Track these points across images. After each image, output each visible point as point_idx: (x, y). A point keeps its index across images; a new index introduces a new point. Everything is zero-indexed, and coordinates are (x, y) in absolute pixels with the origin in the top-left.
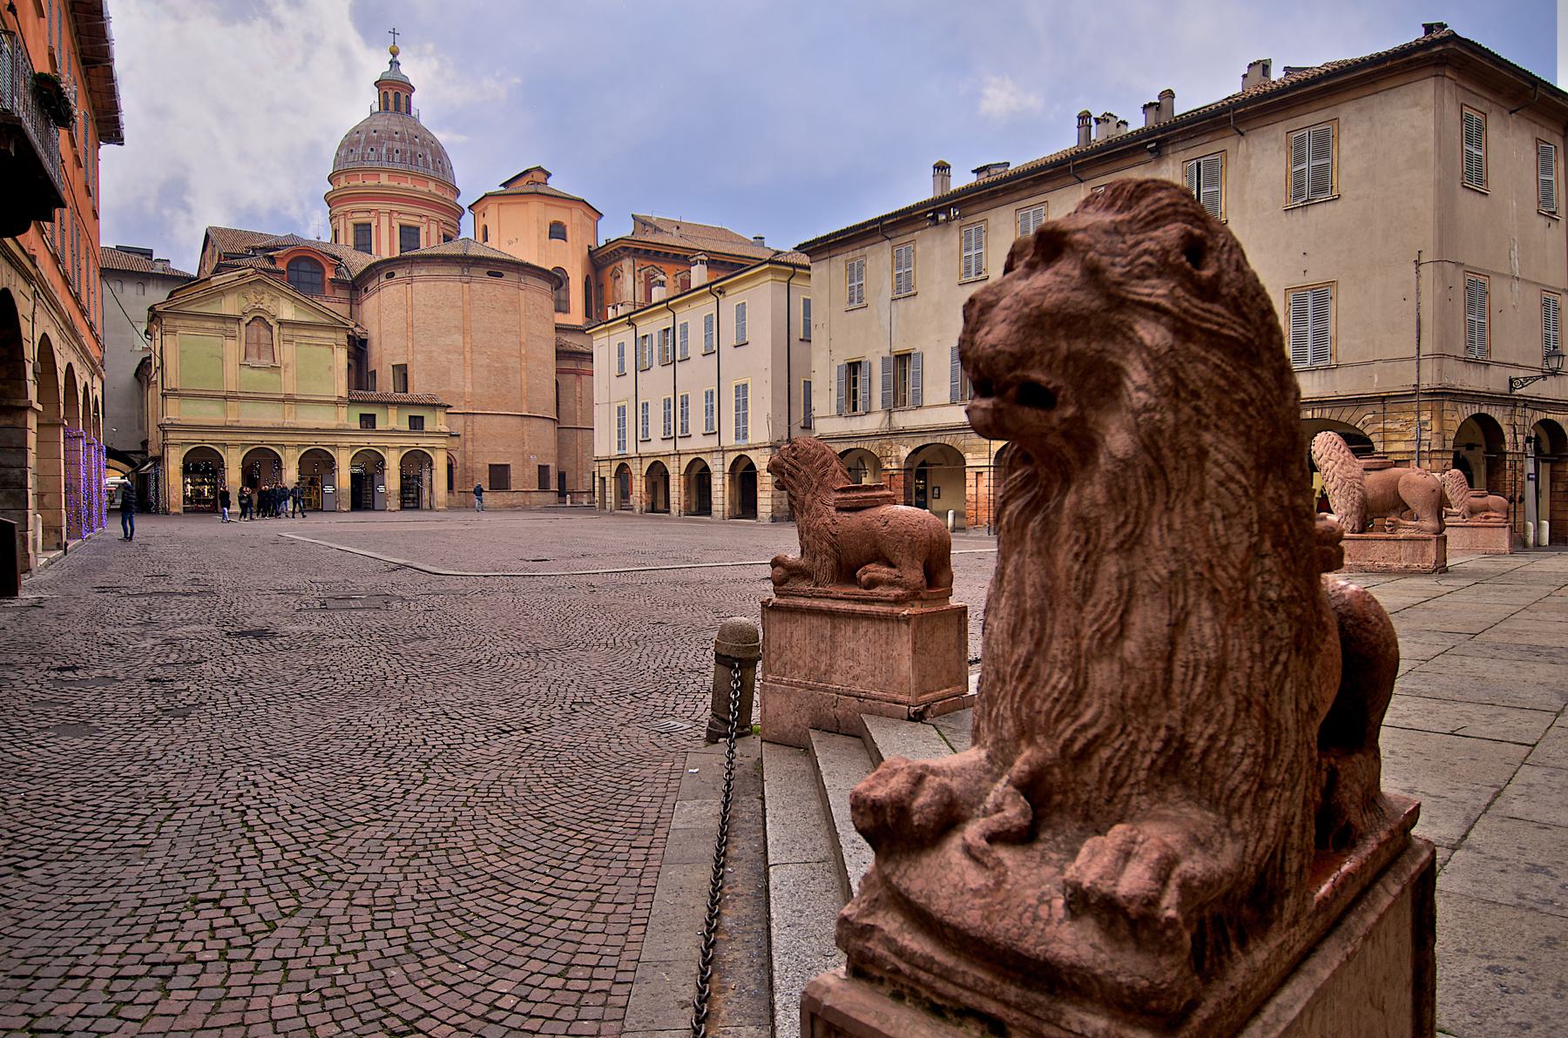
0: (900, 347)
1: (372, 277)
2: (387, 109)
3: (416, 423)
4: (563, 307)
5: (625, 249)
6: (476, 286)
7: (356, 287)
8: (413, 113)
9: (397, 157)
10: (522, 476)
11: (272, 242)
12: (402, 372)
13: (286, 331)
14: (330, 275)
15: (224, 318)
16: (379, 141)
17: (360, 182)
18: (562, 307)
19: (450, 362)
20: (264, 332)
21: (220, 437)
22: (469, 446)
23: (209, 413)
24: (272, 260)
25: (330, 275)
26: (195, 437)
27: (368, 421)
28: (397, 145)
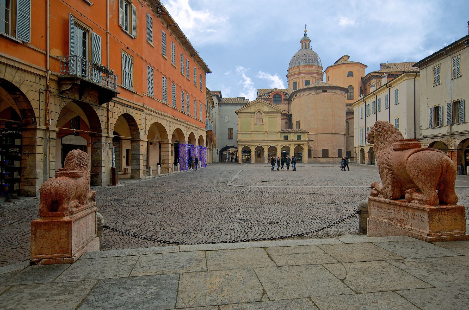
0: (455, 99)
1: (292, 97)
3: (299, 138)
4: (352, 98)
5: (373, 76)
6: (319, 95)
7: (289, 100)
10: (333, 152)
11: (270, 91)
12: (298, 122)
13: (266, 114)
14: (283, 98)
15: (251, 113)
16: (300, 58)
18: (351, 98)
20: (261, 115)
21: (250, 143)
22: (316, 144)
23: (247, 138)
24: (269, 96)
25: (283, 98)
26: (244, 144)
27: (286, 138)
28: (304, 58)
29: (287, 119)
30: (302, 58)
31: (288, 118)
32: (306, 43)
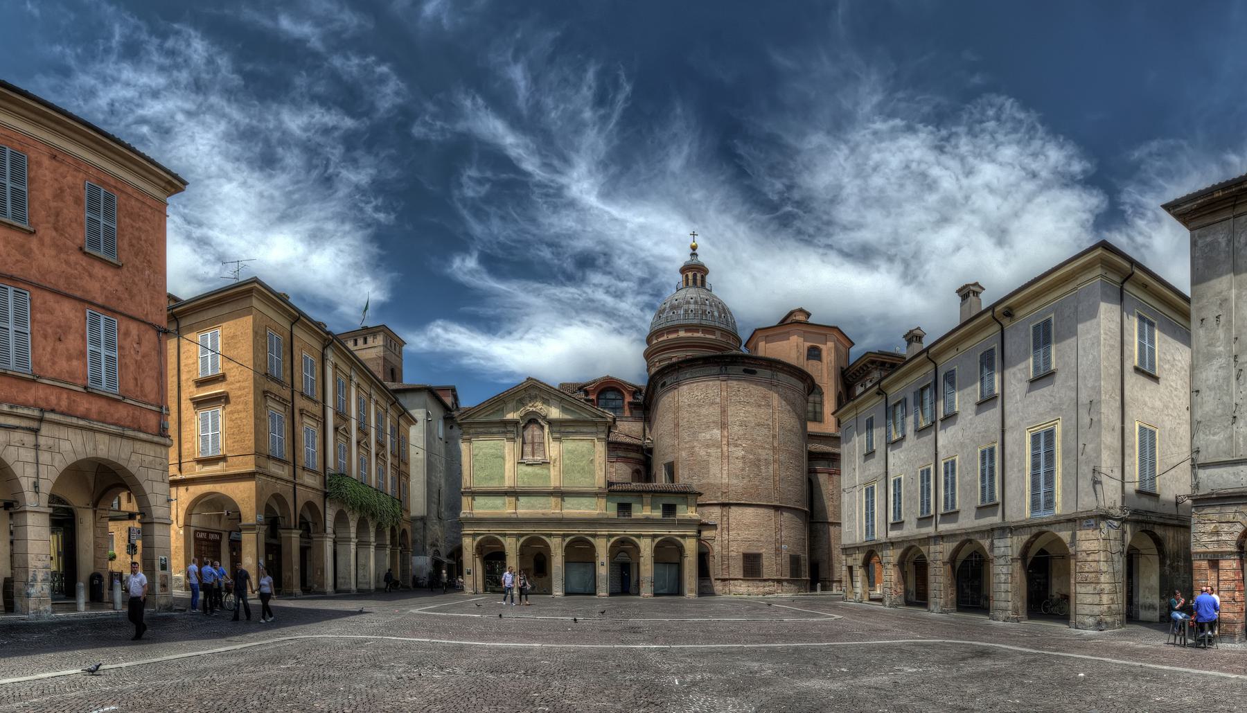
2: (687, 284)
7: (644, 403)
8: (707, 286)
9: (691, 315)
12: (671, 469)
16: (678, 307)
17: (665, 338)
19: (709, 455)
20: (537, 432)
28: (692, 307)
29: (639, 462)
30: (686, 307)
31: (642, 459)
32: (695, 275)
